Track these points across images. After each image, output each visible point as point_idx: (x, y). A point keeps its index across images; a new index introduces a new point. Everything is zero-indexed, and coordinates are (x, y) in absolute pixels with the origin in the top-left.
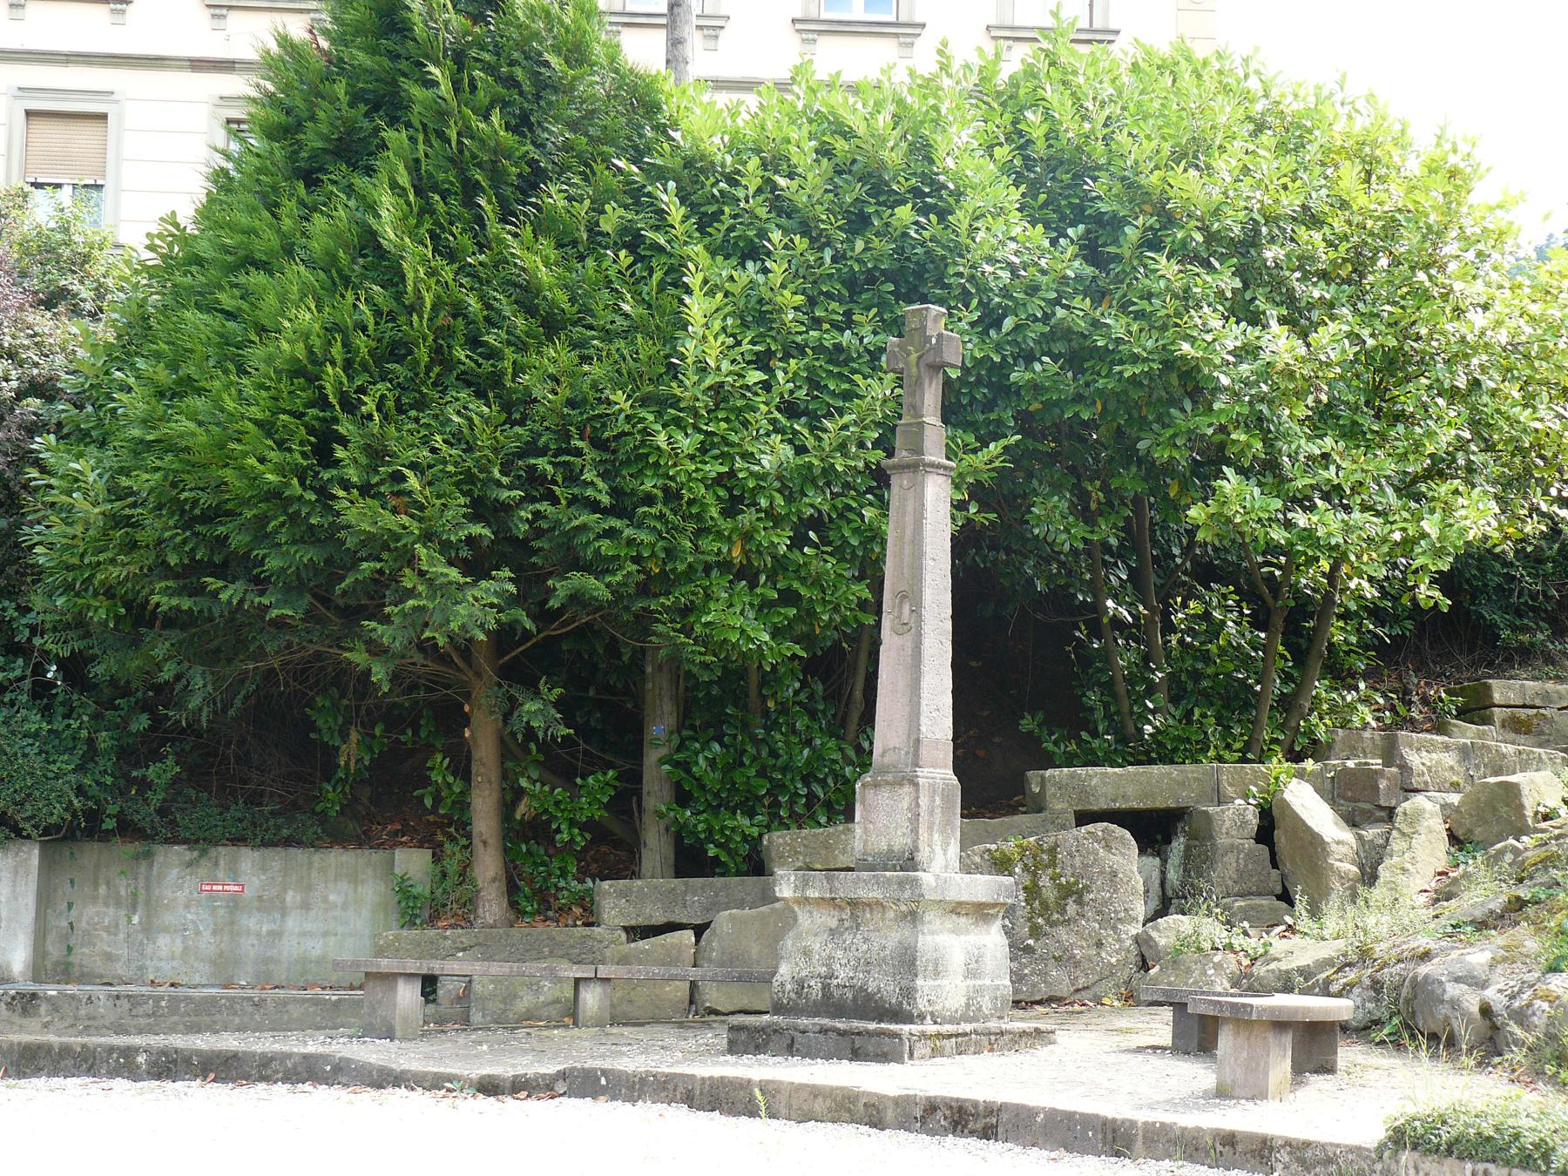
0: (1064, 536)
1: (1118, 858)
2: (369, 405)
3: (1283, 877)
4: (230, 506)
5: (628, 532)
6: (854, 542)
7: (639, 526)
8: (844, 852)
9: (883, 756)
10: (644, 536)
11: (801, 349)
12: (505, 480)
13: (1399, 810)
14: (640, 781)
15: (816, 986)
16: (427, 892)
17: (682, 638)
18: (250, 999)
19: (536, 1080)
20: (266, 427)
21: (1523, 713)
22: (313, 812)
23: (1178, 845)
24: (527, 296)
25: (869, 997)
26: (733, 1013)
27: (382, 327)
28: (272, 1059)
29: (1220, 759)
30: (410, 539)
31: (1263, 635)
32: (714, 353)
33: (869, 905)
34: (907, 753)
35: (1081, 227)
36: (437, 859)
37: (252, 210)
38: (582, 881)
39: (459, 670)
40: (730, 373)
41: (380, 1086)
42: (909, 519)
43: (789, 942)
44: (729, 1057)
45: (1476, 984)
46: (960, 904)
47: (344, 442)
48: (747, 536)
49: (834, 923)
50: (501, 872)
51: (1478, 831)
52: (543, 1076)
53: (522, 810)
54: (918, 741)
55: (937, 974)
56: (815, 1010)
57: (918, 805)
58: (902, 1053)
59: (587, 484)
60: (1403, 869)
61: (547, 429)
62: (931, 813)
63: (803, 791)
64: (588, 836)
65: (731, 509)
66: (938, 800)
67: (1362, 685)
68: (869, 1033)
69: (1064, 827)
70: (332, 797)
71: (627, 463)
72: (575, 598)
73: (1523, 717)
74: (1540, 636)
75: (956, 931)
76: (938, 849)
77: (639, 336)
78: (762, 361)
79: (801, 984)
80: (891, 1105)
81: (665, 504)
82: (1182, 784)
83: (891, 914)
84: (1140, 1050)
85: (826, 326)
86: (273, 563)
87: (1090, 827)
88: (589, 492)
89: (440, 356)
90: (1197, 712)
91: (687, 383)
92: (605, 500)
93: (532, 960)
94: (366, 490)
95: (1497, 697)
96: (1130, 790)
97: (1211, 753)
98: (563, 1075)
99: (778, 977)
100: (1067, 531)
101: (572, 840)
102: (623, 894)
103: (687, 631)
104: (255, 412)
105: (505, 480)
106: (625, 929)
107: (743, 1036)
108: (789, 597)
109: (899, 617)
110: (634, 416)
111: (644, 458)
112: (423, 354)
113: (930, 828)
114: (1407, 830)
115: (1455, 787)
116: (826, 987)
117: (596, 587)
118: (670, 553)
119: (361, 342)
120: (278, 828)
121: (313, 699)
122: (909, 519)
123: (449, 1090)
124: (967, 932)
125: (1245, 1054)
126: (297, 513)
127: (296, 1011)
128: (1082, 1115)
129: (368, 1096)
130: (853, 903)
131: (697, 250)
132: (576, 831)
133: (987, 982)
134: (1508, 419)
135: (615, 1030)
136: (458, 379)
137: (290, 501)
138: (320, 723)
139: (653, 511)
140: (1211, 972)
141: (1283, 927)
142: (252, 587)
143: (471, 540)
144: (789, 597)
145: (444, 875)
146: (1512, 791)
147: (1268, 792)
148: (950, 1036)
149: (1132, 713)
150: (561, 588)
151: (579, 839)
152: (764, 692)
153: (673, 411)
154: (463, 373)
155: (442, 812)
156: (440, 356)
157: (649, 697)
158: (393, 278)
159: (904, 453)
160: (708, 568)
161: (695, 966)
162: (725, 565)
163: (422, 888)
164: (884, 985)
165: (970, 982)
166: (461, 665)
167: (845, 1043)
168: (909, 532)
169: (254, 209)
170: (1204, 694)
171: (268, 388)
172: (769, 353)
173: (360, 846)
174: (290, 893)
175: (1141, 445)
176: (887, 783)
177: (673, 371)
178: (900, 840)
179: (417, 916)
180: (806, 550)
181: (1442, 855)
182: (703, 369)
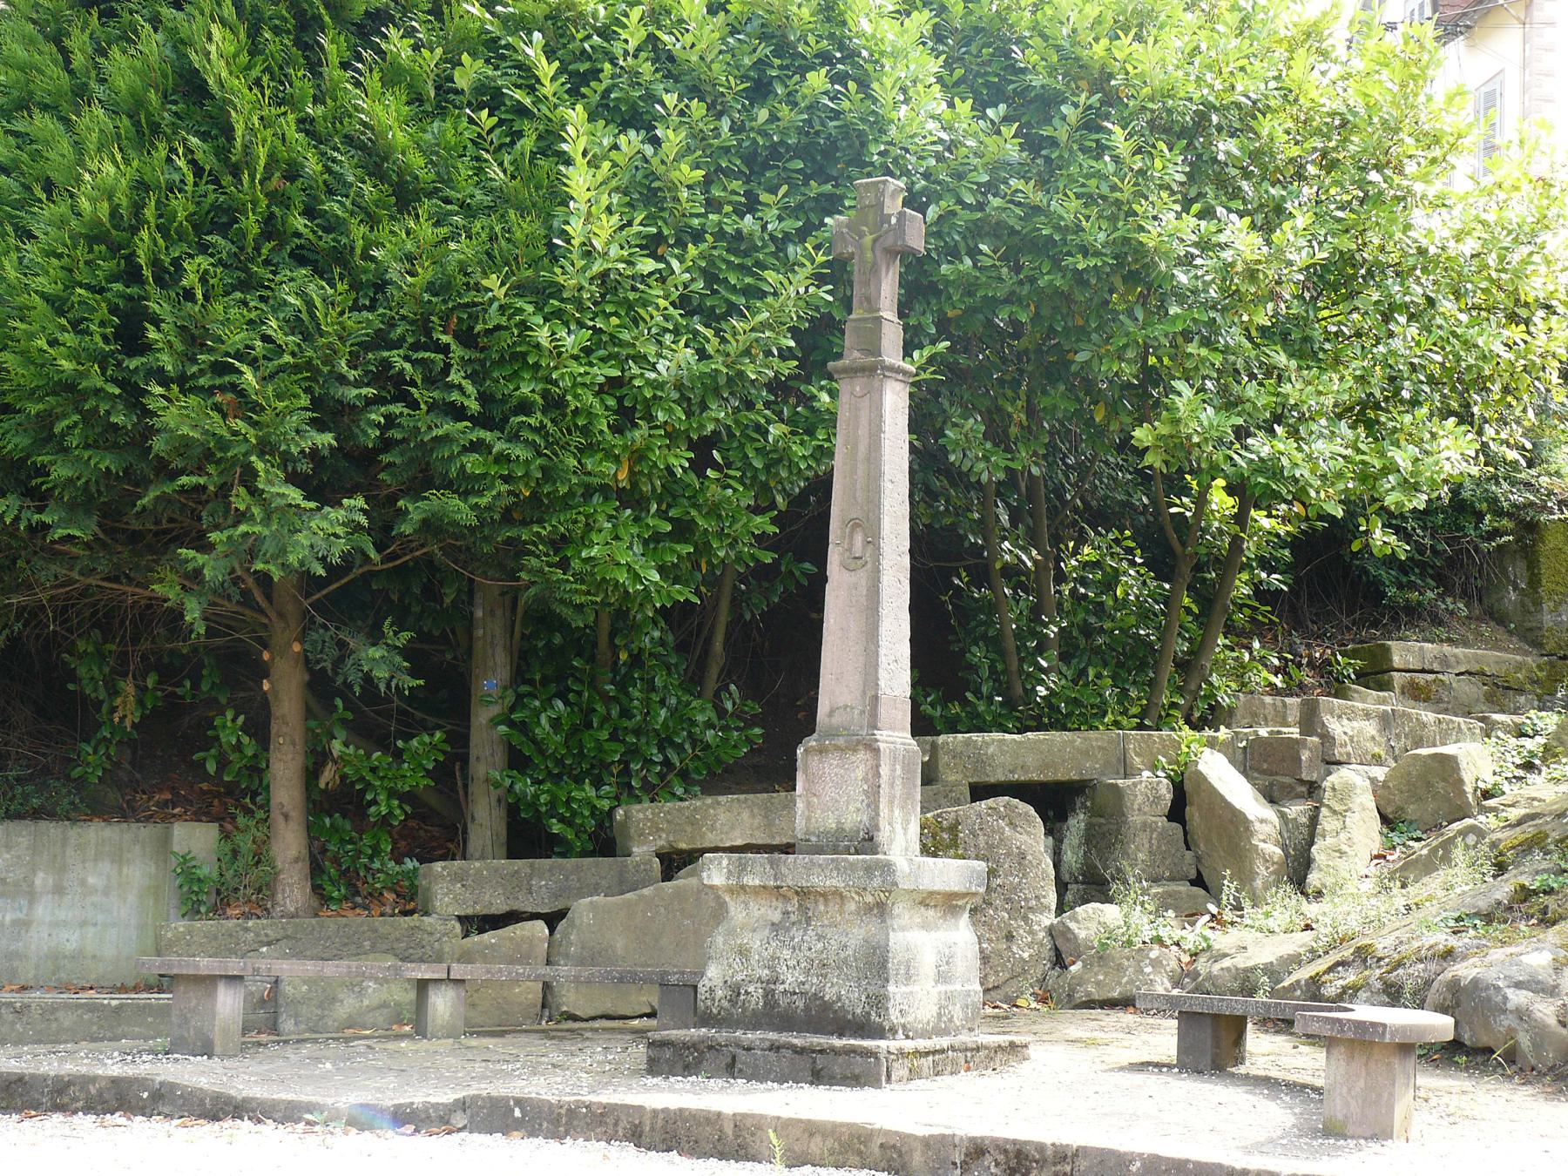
0: (982, 465)
1: (1024, 837)
2: (190, 279)
3: (1198, 858)
4: (9, 399)
5: (499, 447)
6: (758, 464)
7: (514, 437)
8: (712, 828)
9: (831, 713)
10: (519, 451)
11: (698, 237)
12: (352, 374)
13: (1326, 784)
14: (466, 745)
15: (756, 993)
16: (215, 875)
17: (559, 573)
18: (10, 1004)
19: (426, 1110)
20: (58, 305)
21: (1421, 678)
22: (68, 778)
23: (1077, 824)
24: (375, 159)
25: (826, 1006)
26: (593, 1018)
27: (202, 188)
28: (69, 1084)
29: (1117, 724)
30: (243, 448)
31: (1167, 586)
32: (605, 235)
33: (824, 895)
34: (862, 713)
35: (1002, 107)
36: (226, 836)
37: (29, 42)
38: (399, 862)
39: (262, 611)
40: (621, 260)
41: (214, 1117)
42: (863, 432)
43: (720, 940)
44: (651, 1081)
45: (1543, 991)
46: (931, 893)
47: (156, 322)
48: (639, 456)
49: (776, 917)
50: (305, 852)
51: (1411, 809)
52: (436, 1106)
53: (328, 776)
54: (876, 698)
55: (908, 978)
56: (755, 1021)
57: (878, 775)
58: (879, 1075)
59: (451, 387)
60: (1339, 851)
61: (404, 318)
62: (892, 785)
63: (658, 758)
64: (408, 809)
65: (625, 418)
66: (899, 771)
67: (1256, 645)
68: (835, 1051)
69: (958, 802)
70: (92, 760)
71: (501, 362)
72: (430, 526)
73: (1422, 683)
74: (1430, 594)
75: (925, 926)
76: (898, 827)
77: (511, 212)
78: (652, 246)
79: (736, 990)
80: (919, 1147)
81: (544, 412)
82: (1086, 753)
83: (852, 907)
84: (1143, 1066)
85: (728, 209)
86: (61, 471)
87: (991, 802)
88: (455, 396)
89: (271, 229)
90: (1091, 672)
91: (569, 268)
92: (474, 406)
93: (349, 956)
94: (184, 383)
95: (1397, 660)
96: (1030, 760)
97: (1109, 718)
98: (462, 1105)
99: (705, 981)
100: (986, 458)
101: (390, 813)
102: (459, 878)
103: (564, 565)
104: (41, 282)
105: (352, 374)
106: (459, 918)
107: (668, 1053)
108: (683, 530)
109: (849, 550)
110: (509, 306)
111: (520, 359)
112: (251, 224)
113: (891, 802)
114: (1338, 807)
115: (1377, 760)
116: (769, 994)
117: (459, 509)
118: (548, 474)
119: (181, 207)
120: (26, 797)
121: (73, 643)
122: (863, 432)
123: (308, 1123)
124: (937, 928)
125: (1361, 1083)
126: (95, 409)
127: (67, 1019)
128: (1198, 1164)
129: (207, 1129)
130: (803, 893)
131: (576, 116)
132: (396, 803)
133: (958, 987)
134: (1465, 342)
135: (474, 1042)
136: (291, 255)
137: (85, 395)
138: (82, 671)
139: (532, 421)
140: (1148, 970)
141: (1207, 917)
142: (28, 502)
143: (314, 454)
144: (683, 530)
145: (235, 853)
146: (1448, 765)
147: (1177, 763)
148: (927, 1054)
149: (1021, 671)
150: (415, 511)
151: (397, 812)
152: (617, 641)
153: (556, 303)
154: (301, 247)
155: (226, 779)
156: (271, 229)
157: (478, 646)
158: (219, 130)
159: (856, 354)
160: (588, 492)
161: (548, 963)
162: (604, 490)
163: (208, 870)
164: (845, 992)
165: (942, 988)
166: (263, 603)
167: (804, 1063)
168: (862, 448)
169: (32, 41)
170: (1097, 651)
171: (59, 256)
172: (659, 238)
173: (124, 818)
174: (41, 875)
175: (1081, 357)
176: (837, 748)
177: (553, 254)
178: (853, 817)
179: (199, 902)
180: (709, 472)
181: (1377, 838)
182: (588, 253)
